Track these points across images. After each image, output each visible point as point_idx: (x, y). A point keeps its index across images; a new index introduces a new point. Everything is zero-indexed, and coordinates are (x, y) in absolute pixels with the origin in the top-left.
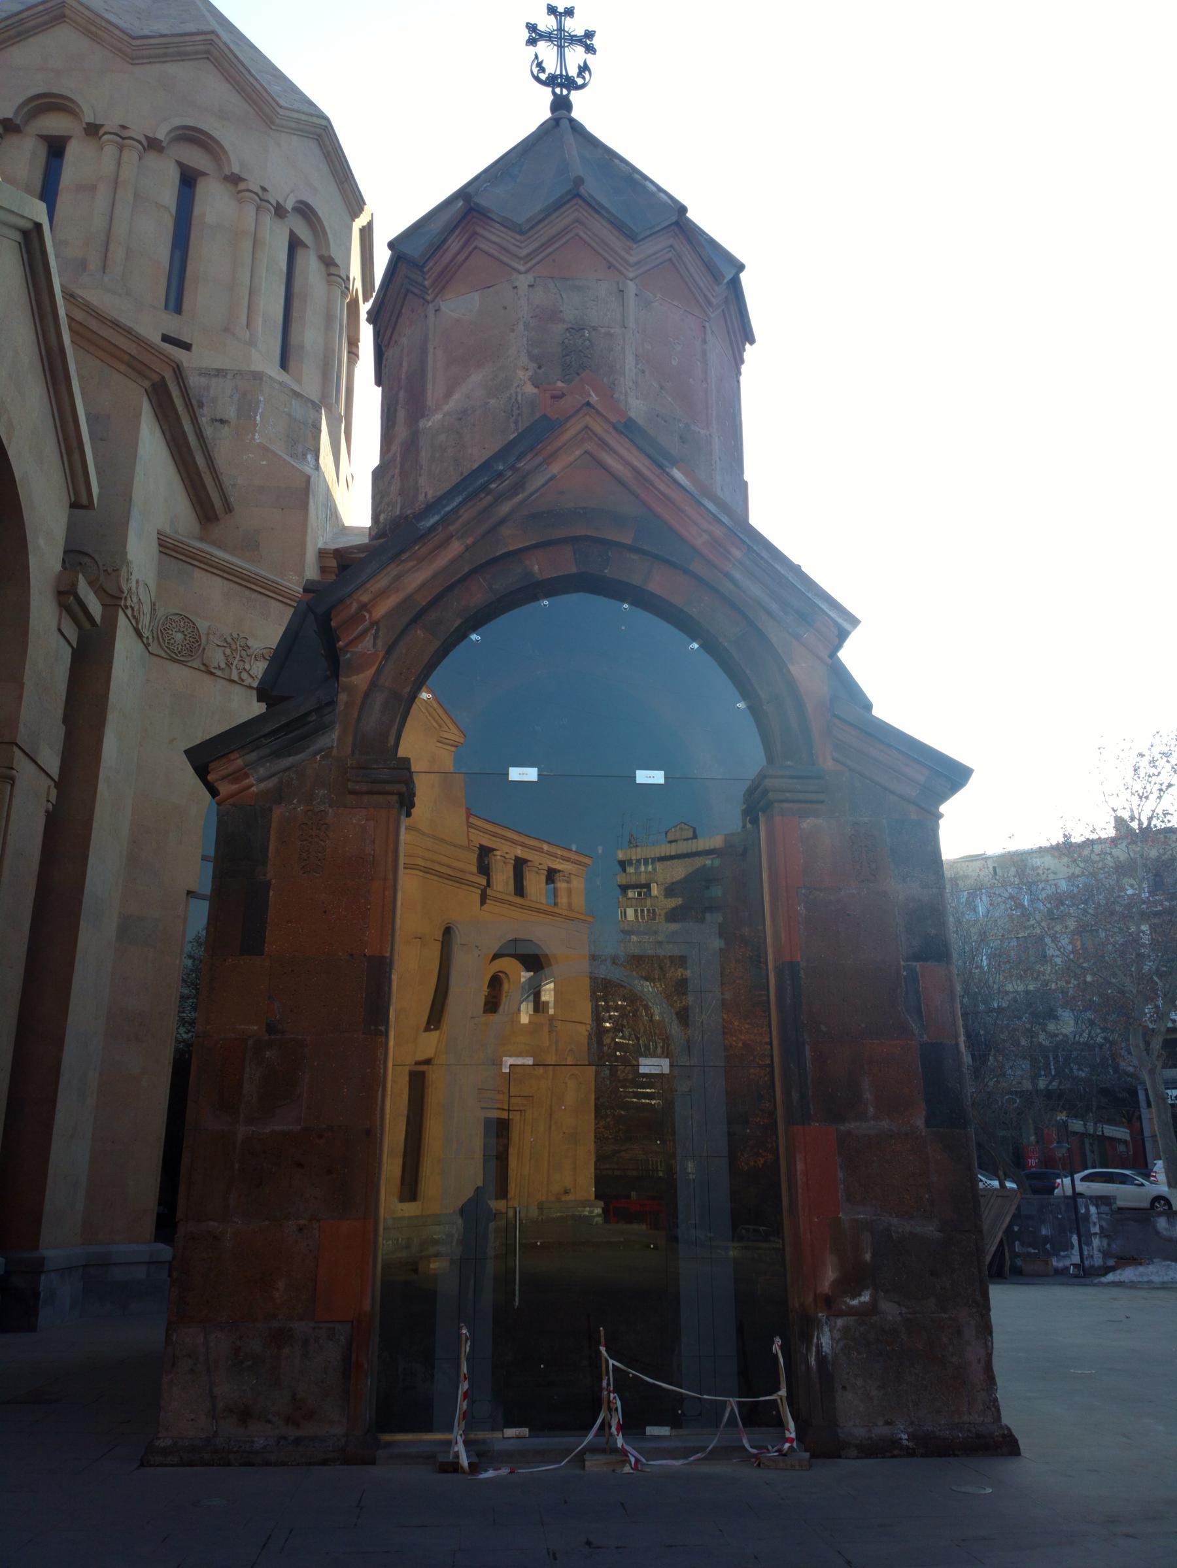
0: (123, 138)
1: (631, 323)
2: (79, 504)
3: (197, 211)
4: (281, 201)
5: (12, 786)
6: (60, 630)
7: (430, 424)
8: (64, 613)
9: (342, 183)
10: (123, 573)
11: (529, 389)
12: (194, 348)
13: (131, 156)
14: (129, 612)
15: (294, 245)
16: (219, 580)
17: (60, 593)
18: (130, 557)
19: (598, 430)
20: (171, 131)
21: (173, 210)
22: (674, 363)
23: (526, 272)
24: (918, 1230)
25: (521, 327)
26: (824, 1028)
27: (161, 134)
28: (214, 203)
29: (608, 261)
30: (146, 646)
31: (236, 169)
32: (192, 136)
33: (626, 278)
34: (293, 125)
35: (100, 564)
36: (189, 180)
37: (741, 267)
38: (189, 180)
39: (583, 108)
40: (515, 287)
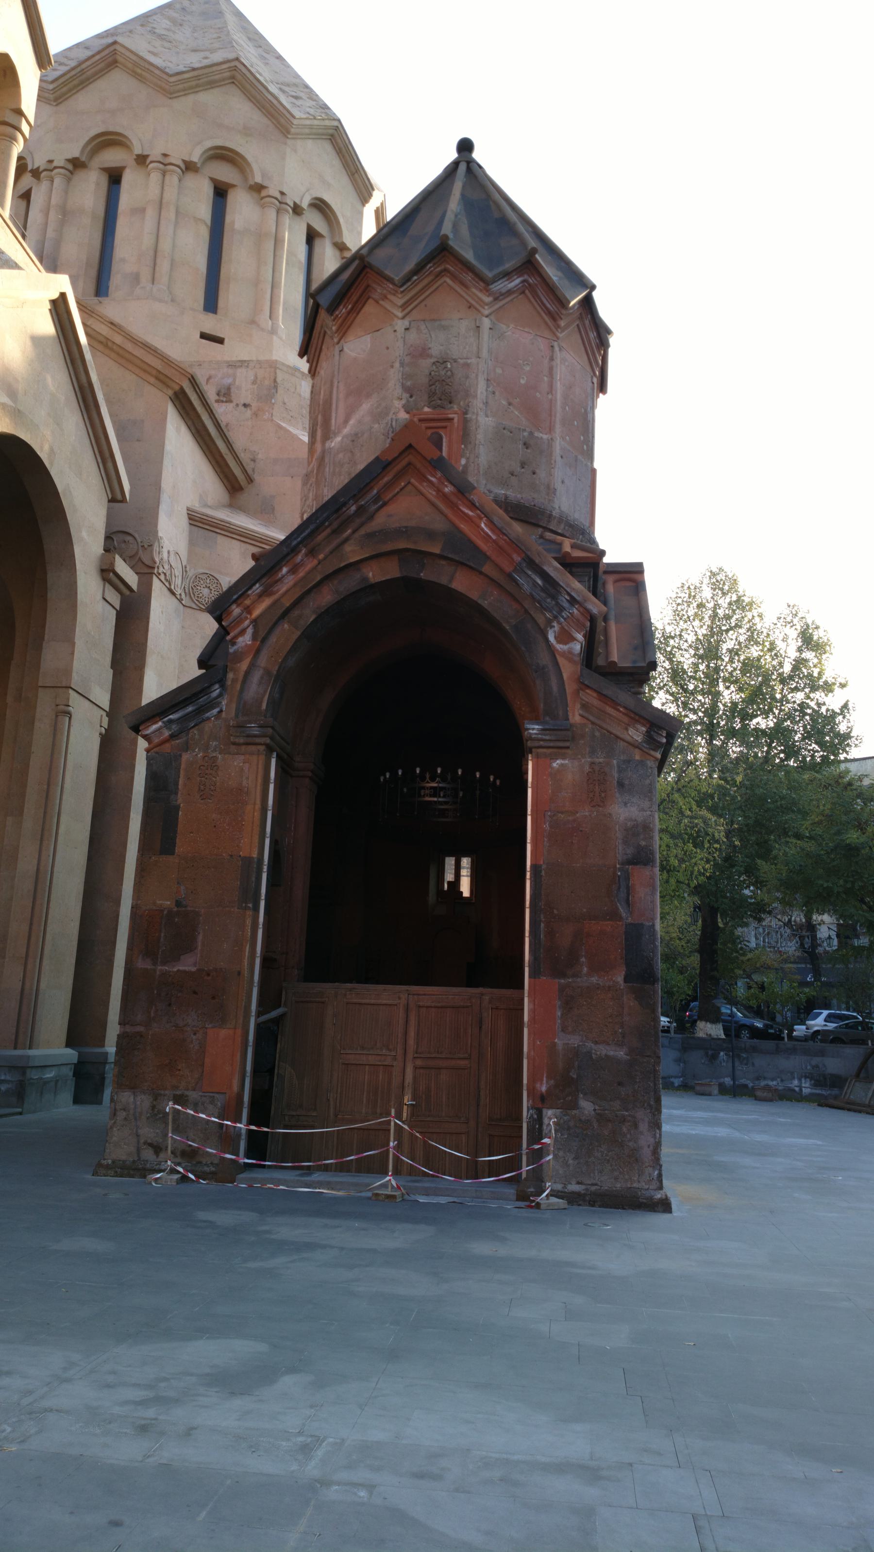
0: (165, 165)
1: (484, 353)
2: (115, 498)
3: (228, 219)
4: (298, 202)
5: (70, 718)
6: (104, 599)
7: (333, 444)
8: (107, 585)
9: (353, 175)
10: (156, 547)
11: (403, 416)
12: (226, 341)
13: (173, 180)
14: (162, 577)
15: (312, 237)
16: (238, 543)
17: (103, 571)
18: (160, 534)
19: (419, 465)
20: (204, 152)
21: (209, 222)
22: (523, 382)
23: (403, 318)
24: (611, 1053)
25: (397, 365)
26: (555, 912)
27: (195, 158)
28: (242, 210)
29: (468, 302)
30: (180, 600)
31: (258, 179)
32: (223, 155)
33: (483, 315)
34: (307, 131)
35: (139, 540)
36: (221, 192)
37: (593, 287)
40: (395, 331)
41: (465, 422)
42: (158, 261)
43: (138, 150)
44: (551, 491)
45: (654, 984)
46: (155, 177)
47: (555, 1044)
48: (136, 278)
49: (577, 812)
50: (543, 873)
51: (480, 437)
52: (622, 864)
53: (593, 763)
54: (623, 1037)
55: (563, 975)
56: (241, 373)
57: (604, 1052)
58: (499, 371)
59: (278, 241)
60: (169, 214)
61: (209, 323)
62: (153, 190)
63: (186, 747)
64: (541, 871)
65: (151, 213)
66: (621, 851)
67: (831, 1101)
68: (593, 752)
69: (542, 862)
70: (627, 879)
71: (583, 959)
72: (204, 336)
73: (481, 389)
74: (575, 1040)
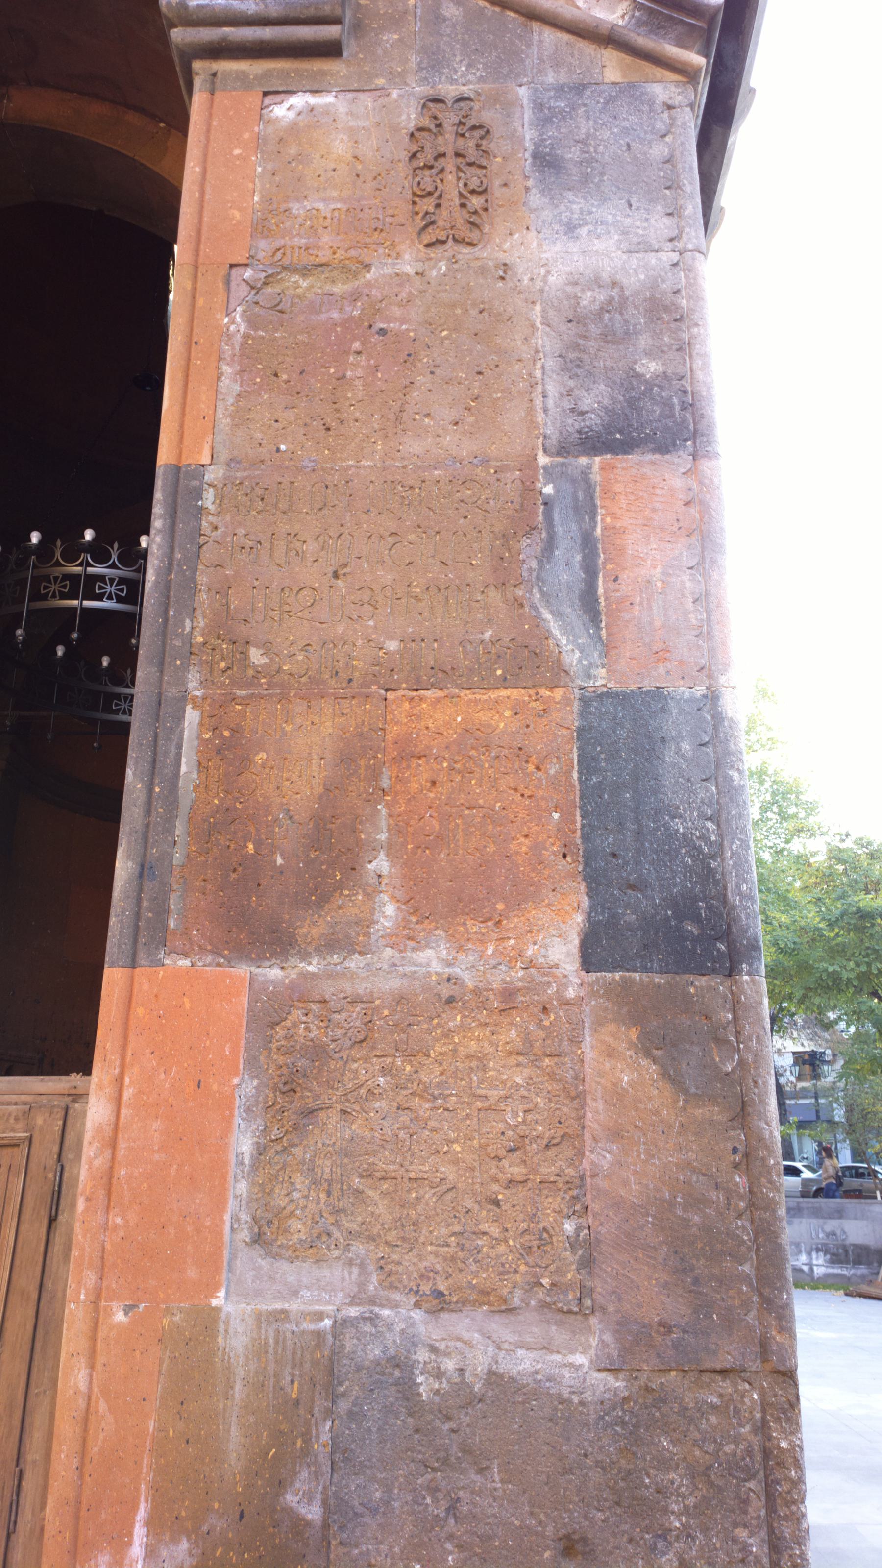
24: (523, 1363)
26: (256, 656)
45: (732, 972)
47: (208, 1322)
49: (367, 267)
50: (209, 499)
52: (562, 450)
53: (436, 100)
54: (587, 1263)
55: (277, 942)
57: (480, 1360)
64: (198, 494)
66: (550, 400)
67: (865, 1288)
68: (434, 62)
69: (205, 459)
70: (586, 509)
71: (381, 864)
74: (318, 1294)
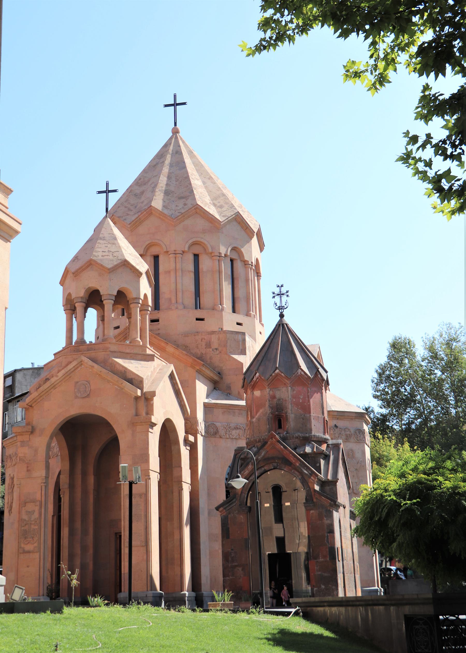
12: (205, 319)
21: (194, 271)
27: (186, 249)
28: (206, 264)
31: (210, 251)
36: (196, 256)
38: (196, 256)
39: (286, 319)
41: (287, 416)
42: (178, 293)
43: (165, 250)
44: (311, 430)
46: (172, 260)
48: (170, 300)
51: (291, 420)
55: (316, 559)
56: (213, 336)
58: (294, 400)
59: (220, 272)
60: (179, 273)
61: (199, 314)
62: (173, 266)
63: (229, 513)
65: (173, 274)
72: (197, 319)
73: (290, 406)
